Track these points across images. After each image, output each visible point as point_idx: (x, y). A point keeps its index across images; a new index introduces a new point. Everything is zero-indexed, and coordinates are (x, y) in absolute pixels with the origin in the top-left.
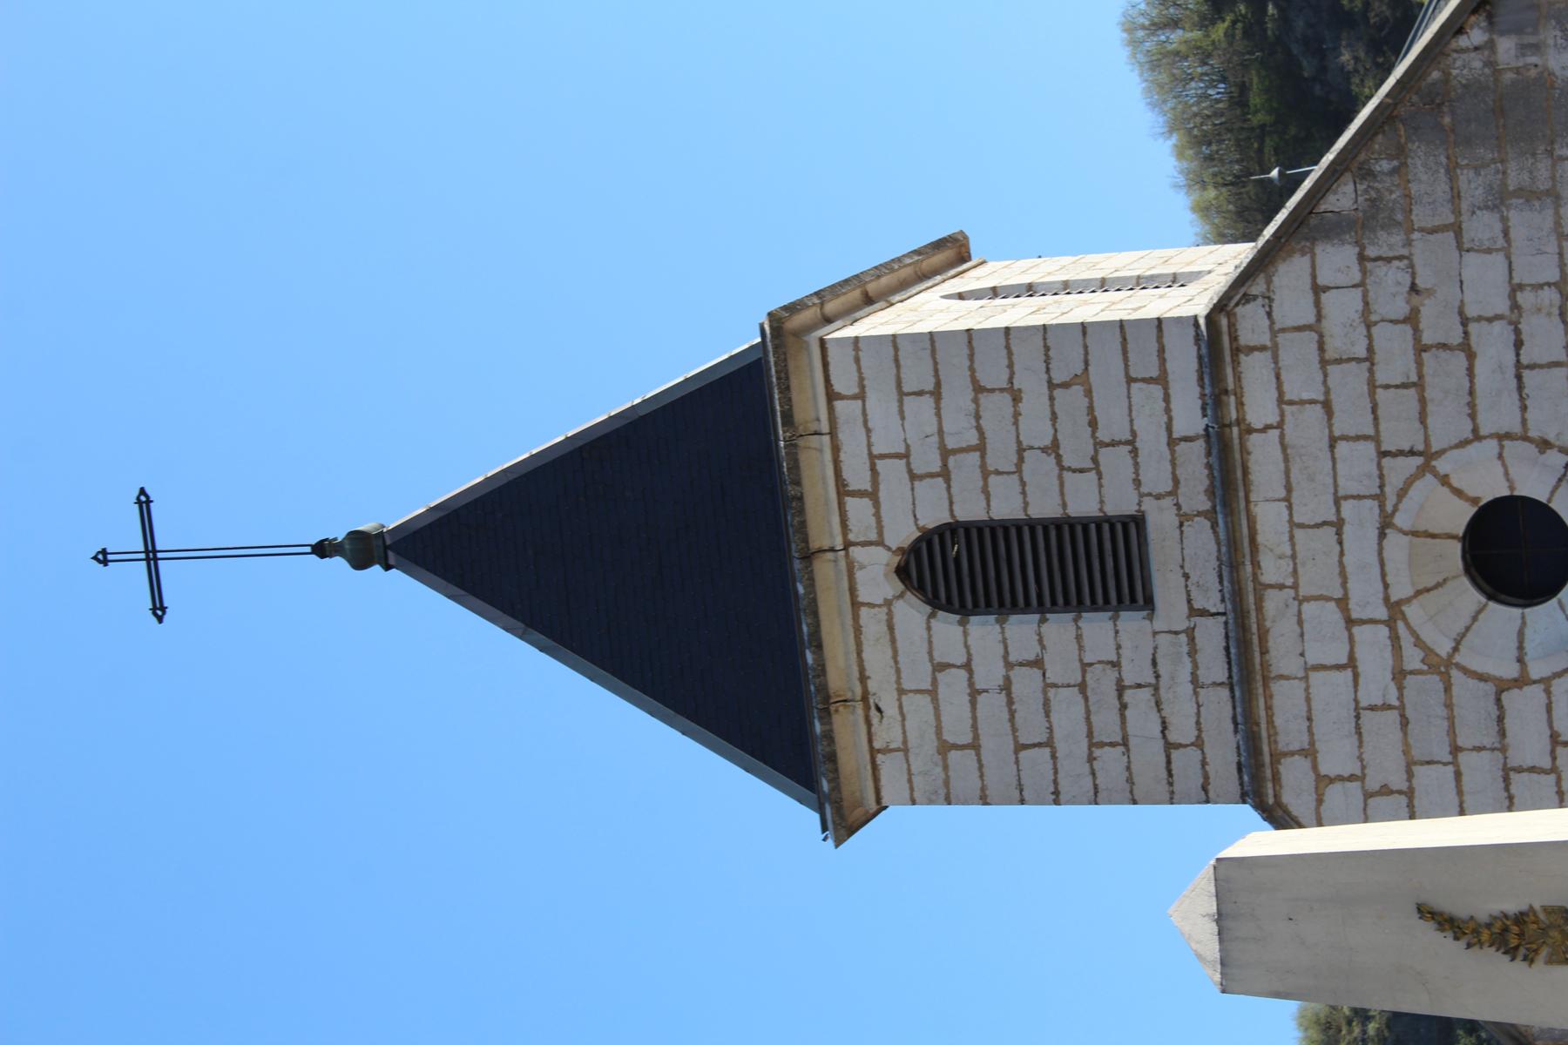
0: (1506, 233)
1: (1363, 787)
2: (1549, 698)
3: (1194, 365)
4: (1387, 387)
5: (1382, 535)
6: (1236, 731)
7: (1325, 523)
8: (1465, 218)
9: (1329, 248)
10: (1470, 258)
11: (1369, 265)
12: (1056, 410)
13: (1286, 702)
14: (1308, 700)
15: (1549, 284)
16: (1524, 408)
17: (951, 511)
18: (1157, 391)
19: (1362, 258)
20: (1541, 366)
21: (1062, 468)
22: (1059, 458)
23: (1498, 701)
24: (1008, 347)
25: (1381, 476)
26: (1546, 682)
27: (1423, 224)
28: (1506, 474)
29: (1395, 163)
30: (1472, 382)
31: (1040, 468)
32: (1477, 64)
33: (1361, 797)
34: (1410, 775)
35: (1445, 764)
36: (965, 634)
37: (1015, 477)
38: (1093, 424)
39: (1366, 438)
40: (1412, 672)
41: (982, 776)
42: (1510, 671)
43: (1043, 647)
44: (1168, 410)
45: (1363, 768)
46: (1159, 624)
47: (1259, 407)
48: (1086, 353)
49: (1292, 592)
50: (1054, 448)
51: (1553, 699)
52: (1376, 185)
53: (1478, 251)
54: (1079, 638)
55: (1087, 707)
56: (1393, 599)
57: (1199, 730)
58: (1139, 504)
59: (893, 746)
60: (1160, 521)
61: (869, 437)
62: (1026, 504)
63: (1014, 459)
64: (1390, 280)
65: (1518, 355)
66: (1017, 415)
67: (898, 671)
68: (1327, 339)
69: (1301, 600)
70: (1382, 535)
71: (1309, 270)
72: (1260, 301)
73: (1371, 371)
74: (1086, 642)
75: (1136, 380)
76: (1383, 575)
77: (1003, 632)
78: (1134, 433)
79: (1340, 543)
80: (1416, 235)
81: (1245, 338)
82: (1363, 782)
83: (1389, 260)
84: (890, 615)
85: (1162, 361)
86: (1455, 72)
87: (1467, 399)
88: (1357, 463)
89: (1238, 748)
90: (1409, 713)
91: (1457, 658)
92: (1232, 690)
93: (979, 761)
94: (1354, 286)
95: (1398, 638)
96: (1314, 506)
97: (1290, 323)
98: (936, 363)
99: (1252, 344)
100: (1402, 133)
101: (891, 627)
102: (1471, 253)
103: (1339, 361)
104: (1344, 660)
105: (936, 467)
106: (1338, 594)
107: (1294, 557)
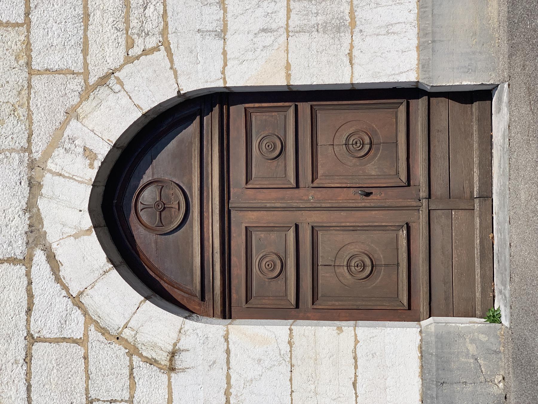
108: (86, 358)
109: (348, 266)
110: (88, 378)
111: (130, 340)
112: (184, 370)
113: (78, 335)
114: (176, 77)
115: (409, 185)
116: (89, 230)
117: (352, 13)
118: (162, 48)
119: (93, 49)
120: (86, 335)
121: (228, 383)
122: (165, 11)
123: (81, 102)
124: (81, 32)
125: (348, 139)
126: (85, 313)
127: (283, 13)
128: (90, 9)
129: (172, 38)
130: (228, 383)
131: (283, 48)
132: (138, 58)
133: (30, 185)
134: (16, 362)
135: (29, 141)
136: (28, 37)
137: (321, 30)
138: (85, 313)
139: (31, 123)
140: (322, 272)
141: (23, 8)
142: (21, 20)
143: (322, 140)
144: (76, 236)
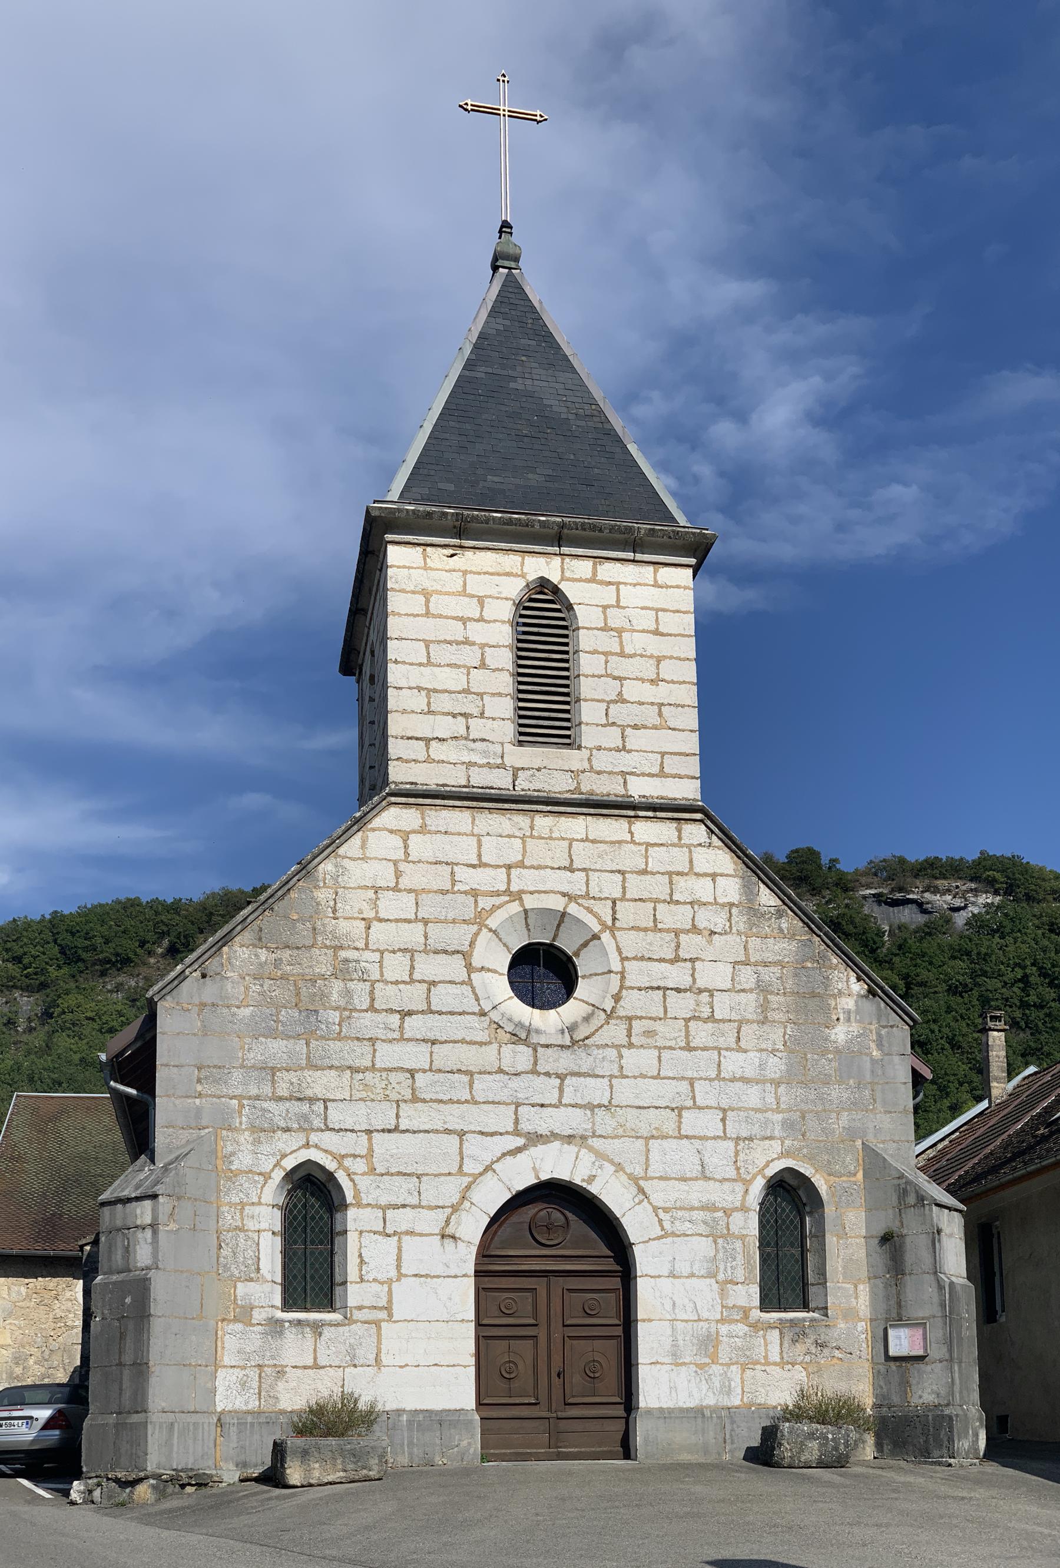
0: (743, 991)
1: (401, 860)
2: (459, 983)
3: (671, 796)
4: (655, 909)
5: (564, 895)
7: (572, 860)
8: (753, 968)
9: (737, 886)
10: (729, 968)
11: (727, 908)
13: (458, 819)
14: (459, 834)
15: (713, 1012)
16: (640, 989)
17: (583, 628)
18: (655, 770)
19: (732, 905)
20: (664, 1002)
21: (609, 702)
22: (616, 702)
23: (458, 952)
24: (684, 682)
25: (600, 899)
26: (469, 982)
27: (750, 943)
28: (596, 974)
29: (786, 932)
30: (657, 960)
31: (610, 690)
32: (840, 986)
33: (393, 858)
34: (410, 891)
35: (416, 914)
36: (503, 622)
37: (603, 672)
38: (635, 727)
39: (624, 893)
40: (476, 901)
42: (476, 962)
43: (494, 670)
44: (643, 775)
45: (414, 862)
46: (508, 748)
47: (647, 830)
48: (679, 730)
49: (528, 834)
50: (621, 700)
51: (458, 986)
52: (773, 919)
53: (733, 973)
54: (500, 695)
55: (454, 692)
56: (523, 896)
57: (438, 762)
58: (585, 747)
59: (428, 560)
60: (574, 759)
61: (631, 584)
62: (587, 676)
63: (616, 674)
64: (719, 921)
65: (672, 989)
66: (643, 680)
67: (479, 573)
68: (685, 878)
69: (523, 838)
70: (564, 895)
71: (726, 872)
72: (708, 841)
73: (664, 901)
74: (497, 699)
75: (662, 757)
77: (503, 646)
78: (629, 751)
79: (559, 868)
80: (744, 939)
81: (688, 828)
82: (404, 861)
83: (729, 920)
84: (516, 575)
85: (674, 776)
86: (836, 972)
87: (647, 956)
89: (426, 785)
90: (450, 896)
91: (485, 930)
92: (465, 787)
93: (418, 615)
94: (715, 898)
95: (499, 895)
96: (583, 855)
97: (695, 856)
98: (675, 635)
99: (683, 831)
101: (508, 574)
102: (732, 969)
103: (671, 883)
104: (484, 860)
105: (611, 623)
106: (527, 863)
107: (551, 838)
108: (449, 1174)
109: (510, 1362)
110: (435, 1175)
111: (463, 1206)
112: (442, 1245)
113: (465, 1169)
114: (643, 1242)
115: (565, 1404)
116: (539, 1178)
117: (684, 1364)
118: (663, 1233)
119: (663, 1184)
120: (466, 1175)
121: (434, 1277)
122: (688, 1235)
123: (627, 1174)
124: (674, 1176)
125: (598, 1362)
126: (481, 1174)
128: (690, 1183)
129: (670, 1239)
130: (434, 1277)
131: (662, 1317)
132: (657, 1215)
133: (570, 1136)
134: (445, 1123)
135: (600, 1136)
136: (671, 1137)
138: (481, 1174)
139: (612, 1138)
140: (505, 1343)
141: (691, 1134)
142: (683, 1132)
143: (597, 1343)
144: (534, 1168)
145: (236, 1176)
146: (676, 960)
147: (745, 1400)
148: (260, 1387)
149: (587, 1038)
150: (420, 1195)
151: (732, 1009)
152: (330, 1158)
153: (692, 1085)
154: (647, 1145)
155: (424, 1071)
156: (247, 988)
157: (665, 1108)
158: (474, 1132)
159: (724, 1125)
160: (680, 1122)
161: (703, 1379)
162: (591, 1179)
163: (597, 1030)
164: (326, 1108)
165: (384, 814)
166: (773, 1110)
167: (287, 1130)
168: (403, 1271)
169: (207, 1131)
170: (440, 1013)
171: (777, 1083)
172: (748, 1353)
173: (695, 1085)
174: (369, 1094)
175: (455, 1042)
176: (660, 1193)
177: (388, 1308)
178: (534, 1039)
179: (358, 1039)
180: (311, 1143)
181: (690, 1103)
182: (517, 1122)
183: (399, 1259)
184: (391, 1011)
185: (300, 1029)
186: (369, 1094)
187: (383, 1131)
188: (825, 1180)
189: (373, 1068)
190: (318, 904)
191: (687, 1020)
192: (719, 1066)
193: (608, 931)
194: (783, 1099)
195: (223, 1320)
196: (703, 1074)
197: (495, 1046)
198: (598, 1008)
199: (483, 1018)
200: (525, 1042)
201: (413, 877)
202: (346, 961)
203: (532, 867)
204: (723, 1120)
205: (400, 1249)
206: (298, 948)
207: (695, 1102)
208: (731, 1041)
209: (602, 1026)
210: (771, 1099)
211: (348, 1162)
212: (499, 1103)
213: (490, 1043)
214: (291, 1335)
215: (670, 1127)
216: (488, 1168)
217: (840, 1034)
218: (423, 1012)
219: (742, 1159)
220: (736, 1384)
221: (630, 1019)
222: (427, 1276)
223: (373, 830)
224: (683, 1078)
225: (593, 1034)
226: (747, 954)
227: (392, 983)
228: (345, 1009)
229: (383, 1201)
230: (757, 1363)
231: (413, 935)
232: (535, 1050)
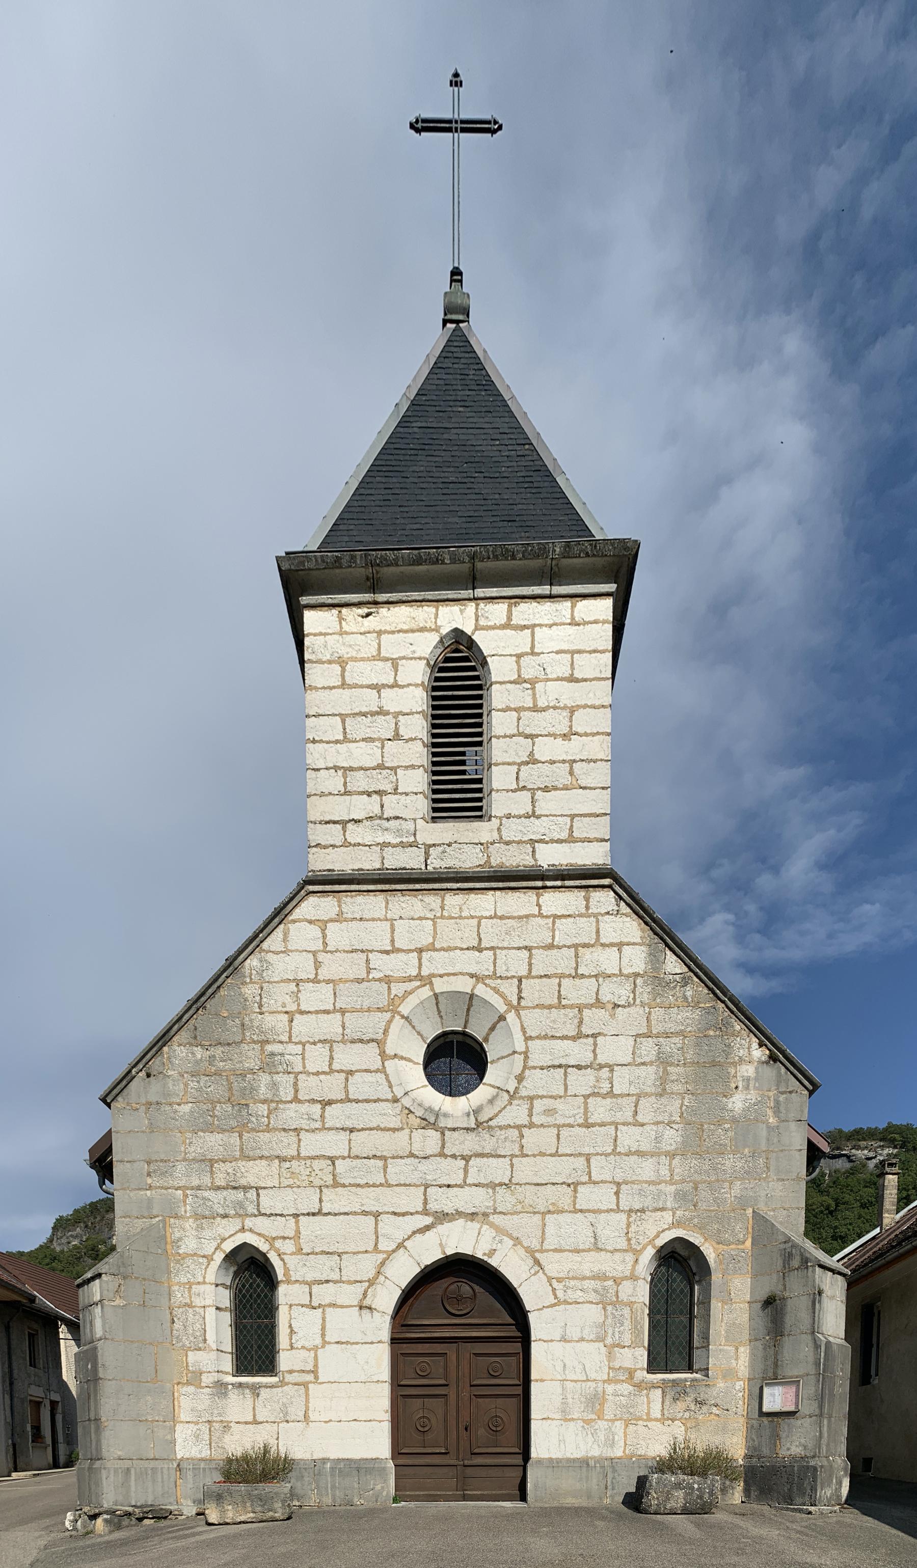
0: (643, 1064)
5: (472, 976)
6: (353, 870)
7: (480, 939)
8: (655, 1040)
9: (644, 955)
10: (631, 1041)
12: (557, 765)
15: (612, 1087)
16: (542, 1068)
19: (637, 975)
20: (565, 1080)
21: (520, 765)
26: (383, 1070)
27: (653, 1014)
34: (328, 982)
35: (334, 1004)
39: (530, 970)
41: (324, 688)
45: (331, 952)
46: (420, 823)
48: (591, 788)
49: (439, 915)
50: (532, 760)
52: (678, 988)
57: (355, 845)
60: (483, 831)
61: (546, 626)
64: (623, 993)
65: (573, 1066)
70: (472, 976)
72: (616, 908)
75: (572, 821)
76: (448, 975)
79: (468, 949)
85: (583, 840)
86: (738, 1039)
88: (516, 963)
91: (397, 1017)
96: (491, 933)
100: (707, 1005)
107: (460, 917)
108: (366, 1252)
110: (354, 1253)
117: (573, 1419)
118: (556, 1301)
121: (353, 1343)
126: (394, 1251)
127: (575, 1378)
129: (562, 1307)
130: (353, 1343)
132: (551, 1285)
133: (473, 1214)
135: (500, 1213)
136: (567, 1211)
137: (564, 1401)
138: (394, 1251)
139: (512, 1214)
142: (578, 1207)
145: (183, 1259)
146: (579, 1036)
147: (627, 1452)
148: (210, 1439)
149: (491, 1119)
150: (341, 1271)
151: (631, 1083)
152: (263, 1240)
153: (588, 1161)
154: (543, 1219)
155: (344, 1158)
156: (186, 1085)
157: (562, 1184)
158: (388, 1213)
159: (618, 1199)
160: (575, 1197)
161: (589, 1433)
162: (492, 1252)
163: (500, 1111)
164: (258, 1195)
165: (304, 905)
166: (666, 1182)
167: (225, 1216)
168: (327, 1339)
169: (157, 1219)
170: (357, 1101)
171: (671, 1155)
172: (631, 1410)
173: (591, 1160)
174: (296, 1181)
175: (371, 1129)
176: (554, 1265)
177: (315, 1372)
178: (442, 1123)
179: (284, 1130)
180: (246, 1228)
181: (585, 1178)
182: (425, 1202)
183: (323, 1328)
184: (313, 1101)
185: (233, 1123)
186: (296, 1181)
187: (308, 1214)
188: (714, 1248)
189: (298, 1157)
190: (246, 1000)
191: (586, 1097)
192: (615, 1140)
193: (513, 1011)
194: (677, 1171)
195: (178, 1383)
196: (599, 1150)
197: (407, 1131)
198: (502, 1090)
199: (396, 1105)
200: (434, 1126)
201: (332, 967)
202: (272, 1054)
203: (443, 949)
204: (617, 1194)
205: (324, 1319)
206: (229, 1044)
207: (590, 1177)
208: (628, 1115)
209: (505, 1107)
210: (665, 1172)
211: (278, 1244)
212: (410, 1185)
213: (402, 1129)
214: (233, 1395)
215: (566, 1202)
216: (400, 1246)
217: (737, 1103)
218: (341, 1101)
219: (633, 1231)
220: (619, 1438)
221: (531, 1099)
222: (347, 1343)
223: (294, 921)
224: (580, 1154)
225: (496, 1115)
226: (649, 1026)
227: (313, 1074)
228: (272, 1101)
229: (309, 1278)
230: (640, 1419)
231: (330, 1026)
232: (443, 1134)
